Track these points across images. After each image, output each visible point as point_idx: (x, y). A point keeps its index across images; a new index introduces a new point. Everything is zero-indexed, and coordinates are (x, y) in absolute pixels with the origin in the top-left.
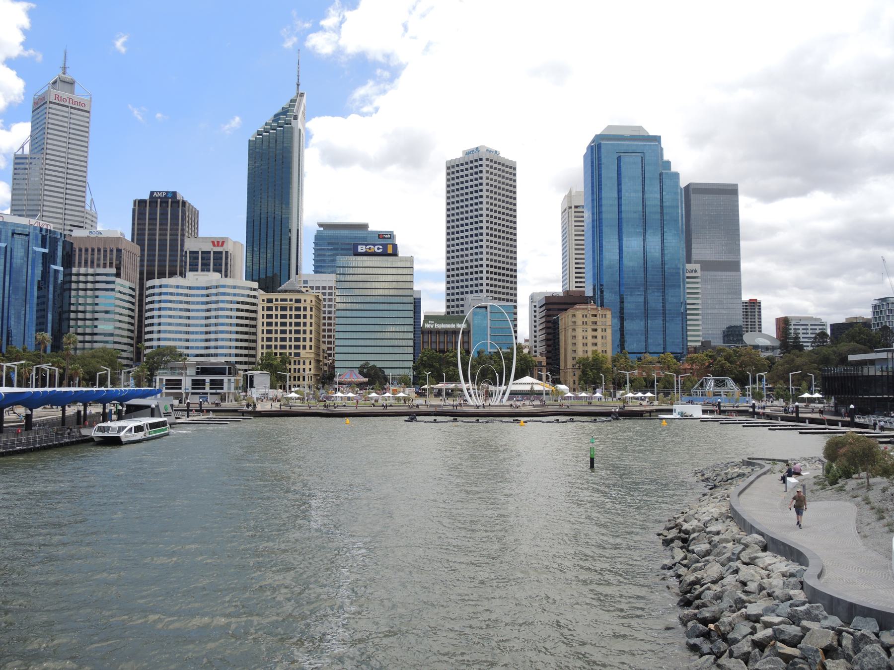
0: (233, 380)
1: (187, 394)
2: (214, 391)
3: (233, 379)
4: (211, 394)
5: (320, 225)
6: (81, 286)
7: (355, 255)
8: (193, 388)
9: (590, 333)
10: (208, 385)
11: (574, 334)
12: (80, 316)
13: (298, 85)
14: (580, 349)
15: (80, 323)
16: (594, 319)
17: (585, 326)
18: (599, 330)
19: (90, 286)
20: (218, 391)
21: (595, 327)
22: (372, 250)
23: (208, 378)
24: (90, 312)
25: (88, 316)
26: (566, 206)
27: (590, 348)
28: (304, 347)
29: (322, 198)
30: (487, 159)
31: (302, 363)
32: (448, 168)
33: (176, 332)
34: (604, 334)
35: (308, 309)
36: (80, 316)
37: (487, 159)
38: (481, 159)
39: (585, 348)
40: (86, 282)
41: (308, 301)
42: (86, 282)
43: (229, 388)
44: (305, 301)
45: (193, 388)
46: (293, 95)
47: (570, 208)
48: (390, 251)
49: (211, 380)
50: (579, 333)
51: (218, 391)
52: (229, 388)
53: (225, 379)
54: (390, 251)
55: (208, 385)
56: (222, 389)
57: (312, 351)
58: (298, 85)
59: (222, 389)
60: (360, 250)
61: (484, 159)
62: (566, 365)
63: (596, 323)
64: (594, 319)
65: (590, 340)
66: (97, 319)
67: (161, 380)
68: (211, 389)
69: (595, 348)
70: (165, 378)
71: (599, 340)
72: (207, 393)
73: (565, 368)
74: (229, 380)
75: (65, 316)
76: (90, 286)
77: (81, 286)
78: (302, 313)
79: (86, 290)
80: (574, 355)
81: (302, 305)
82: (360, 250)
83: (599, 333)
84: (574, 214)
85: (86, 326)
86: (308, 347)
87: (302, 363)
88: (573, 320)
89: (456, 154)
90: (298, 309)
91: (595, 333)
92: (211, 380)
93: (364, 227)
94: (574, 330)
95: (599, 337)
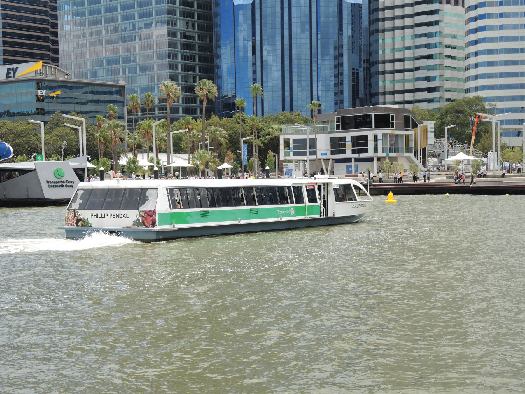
0: (380, 137)
1: (326, 161)
2: (356, 155)
3: (380, 132)
4: (357, 160)
6: (398, 23)
8: (333, 153)
10: (349, 145)
12: (398, 66)
15: (398, 76)
19: (408, 21)
20: (363, 155)
23: (349, 135)
24: (410, 59)
25: (408, 65)
33: (501, 75)
36: (398, 66)
40: (403, 17)
42: (403, 17)
43: (376, 150)
45: (333, 153)
49: (353, 138)
51: (363, 155)
52: (376, 150)
53: (370, 133)
55: (349, 145)
56: (366, 151)
59: (366, 151)
66: (418, 69)
67: (287, 143)
68: (354, 152)
70: (291, 138)
72: (349, 160)
74: (376, 136)
75: (373, 69)
76: (408, 21)
77: (398, 23)
79: (403, 28)
85: (404, 81)
92: (353, 138)
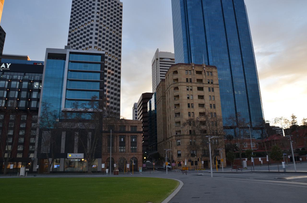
9: (196, 93)
11: (176, 93)
14: (185, 110)
16: (199, 77)
17: (190, 84)
18: (206, 89)
21: (201, 85)
26: (155, 59)
27: (197, 110)
34: (211, 93)
39: (191, 110)
47: (157, 59)
50: (183, 91)
62: (165, 132)
63: (200, 81)
64: (199, 77)
65: (196, 101)
69: (202, 110)
71: (207, 101)
73: (166, 139)
80: (177, 119)
83: (206, 92)
84: (159, 62)
88: (175, 77)
91: (201, 93)
94: (176, 88)
95: (207, 98)
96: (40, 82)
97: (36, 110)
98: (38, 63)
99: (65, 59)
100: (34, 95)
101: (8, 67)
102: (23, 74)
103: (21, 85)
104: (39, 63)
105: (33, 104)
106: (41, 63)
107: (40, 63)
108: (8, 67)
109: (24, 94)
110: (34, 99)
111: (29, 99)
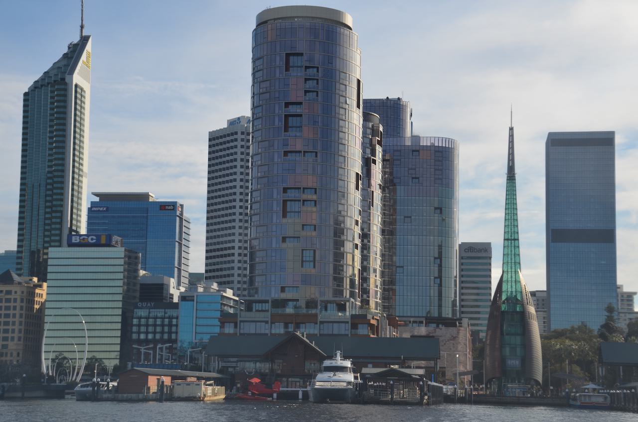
5: (97, 195)
7: (71, 245)
13: (82, 27)
22: (86, 241)
28: (13, 339)
29: (103, 165)
30: (243, 133)
31: (9, 355)
32: (210, 140)
35: (19, 300)
37: (243, 133)
38: (236, 133)
41: (19, 293)
44: (16, 292)
46: (76, 39)
48: (103, 241)
54: (103, 241)
57: (21, 342)
58: (82, 27)
60: (73, 241)
61: (239, 133)
78: (12, 304)
81: (12, 297)
82: (73, 241)
86: (16, 339)
87: (9, 355)
89: (221, 124)
90: (8, 301)
93: (145, 196)
96: (177, 318)
97: (175, 341)
98: (167, 206)
99: (193, 301)
100: (174, 329)
101: (153, 305)
102: (163, 310)
103: (163, 322)
104: (168, 206)
105: (173, 336)
106: (172, 206)
107: (170, 206)
108: (153, 305)
109: (166, 329)
110: (174, 333)
111: (170, 333)
